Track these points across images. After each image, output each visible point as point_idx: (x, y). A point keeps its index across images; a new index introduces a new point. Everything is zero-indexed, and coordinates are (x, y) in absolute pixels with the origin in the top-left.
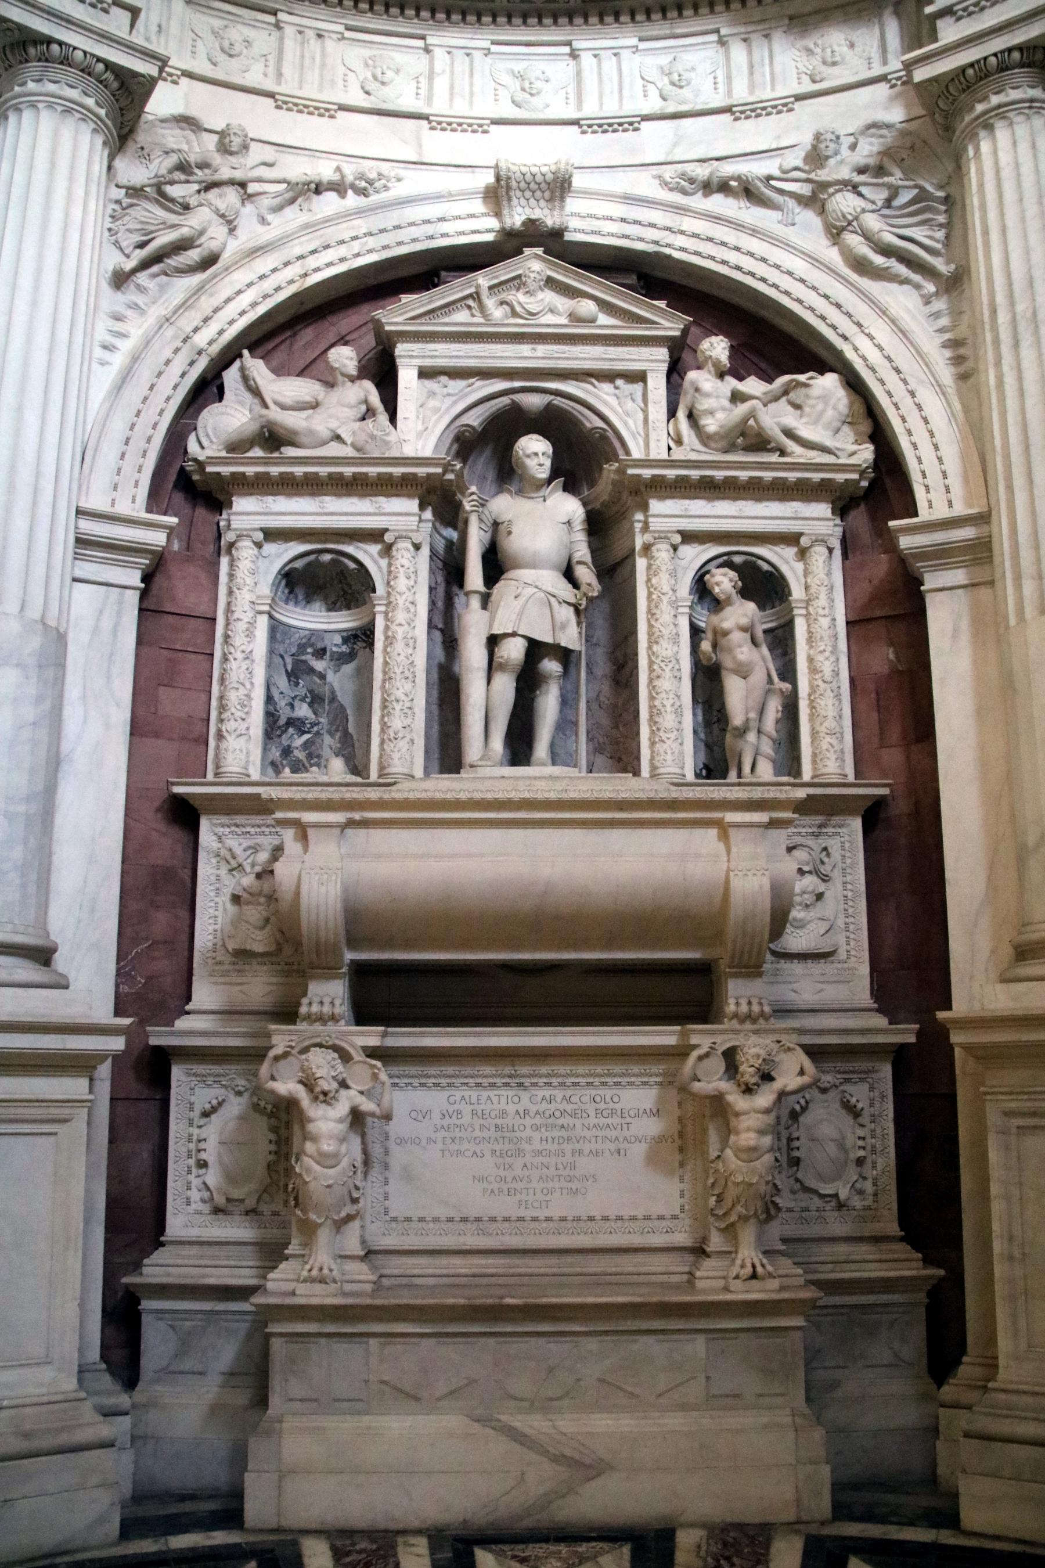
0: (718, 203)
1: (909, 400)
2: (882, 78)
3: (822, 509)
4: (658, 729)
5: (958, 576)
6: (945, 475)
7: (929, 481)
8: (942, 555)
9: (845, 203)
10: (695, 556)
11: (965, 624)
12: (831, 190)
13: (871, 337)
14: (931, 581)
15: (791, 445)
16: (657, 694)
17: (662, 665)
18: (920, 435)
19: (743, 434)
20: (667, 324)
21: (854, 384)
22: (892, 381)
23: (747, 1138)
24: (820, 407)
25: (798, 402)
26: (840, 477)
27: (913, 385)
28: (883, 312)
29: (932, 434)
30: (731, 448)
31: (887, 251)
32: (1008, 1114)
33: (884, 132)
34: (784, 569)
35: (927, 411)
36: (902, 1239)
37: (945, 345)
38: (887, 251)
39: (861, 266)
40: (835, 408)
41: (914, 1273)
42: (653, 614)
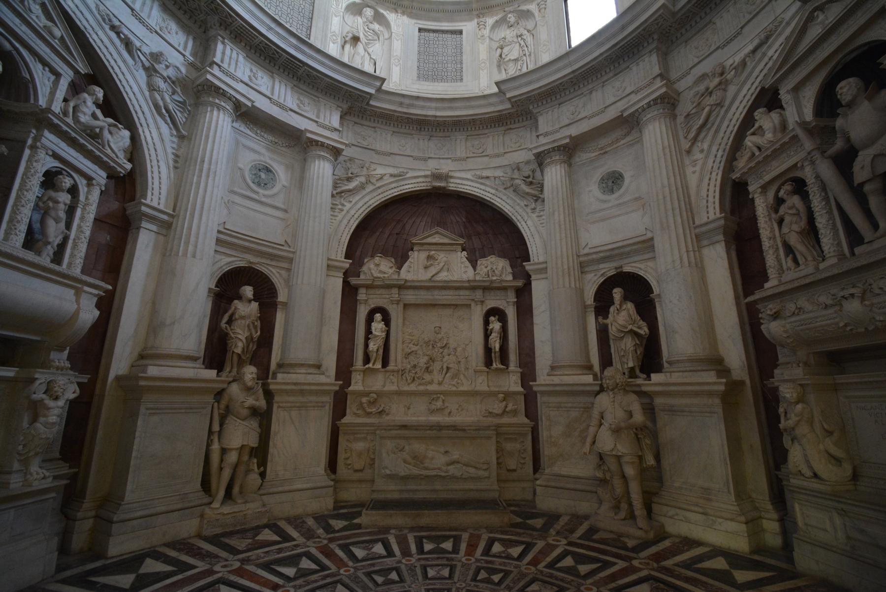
0: (113, 35)
1: (156, 161)
2: (184, 56)
3: (104, 174)
4: (16, 229)
5: (154, 228)
6: (160, 194)
7: (154, 192)
8: (152, 219)
9: (162, 85)
10: (54, 164)
11: (151, 244)
12: (158, 75)
13: (151, 133)
14: (144, 224)
15: (107, 147)
16: (20, 213)
17: (27, 202)
18: (156, 175)
19: (91, 130)
20: (81, 66)
21: (135, 139)
22: (152, 152)
23: (53, 419)
24: (120, 139)
25: (113, 132)
26: (119, 169)
27: (159, 158)
28: (158, 128)
29: (160, 178)
30: (84, 131)
31: (168, 111)
32: (147, 409)
33: (179, 72)
34: (80, 187)
35: (161, 170)
36: (59, 459)
37: (173, 154)
38: (168, 111)
39: (157, 107)
40: (124, 143)
41: (66, 472)
42: (29, 178)
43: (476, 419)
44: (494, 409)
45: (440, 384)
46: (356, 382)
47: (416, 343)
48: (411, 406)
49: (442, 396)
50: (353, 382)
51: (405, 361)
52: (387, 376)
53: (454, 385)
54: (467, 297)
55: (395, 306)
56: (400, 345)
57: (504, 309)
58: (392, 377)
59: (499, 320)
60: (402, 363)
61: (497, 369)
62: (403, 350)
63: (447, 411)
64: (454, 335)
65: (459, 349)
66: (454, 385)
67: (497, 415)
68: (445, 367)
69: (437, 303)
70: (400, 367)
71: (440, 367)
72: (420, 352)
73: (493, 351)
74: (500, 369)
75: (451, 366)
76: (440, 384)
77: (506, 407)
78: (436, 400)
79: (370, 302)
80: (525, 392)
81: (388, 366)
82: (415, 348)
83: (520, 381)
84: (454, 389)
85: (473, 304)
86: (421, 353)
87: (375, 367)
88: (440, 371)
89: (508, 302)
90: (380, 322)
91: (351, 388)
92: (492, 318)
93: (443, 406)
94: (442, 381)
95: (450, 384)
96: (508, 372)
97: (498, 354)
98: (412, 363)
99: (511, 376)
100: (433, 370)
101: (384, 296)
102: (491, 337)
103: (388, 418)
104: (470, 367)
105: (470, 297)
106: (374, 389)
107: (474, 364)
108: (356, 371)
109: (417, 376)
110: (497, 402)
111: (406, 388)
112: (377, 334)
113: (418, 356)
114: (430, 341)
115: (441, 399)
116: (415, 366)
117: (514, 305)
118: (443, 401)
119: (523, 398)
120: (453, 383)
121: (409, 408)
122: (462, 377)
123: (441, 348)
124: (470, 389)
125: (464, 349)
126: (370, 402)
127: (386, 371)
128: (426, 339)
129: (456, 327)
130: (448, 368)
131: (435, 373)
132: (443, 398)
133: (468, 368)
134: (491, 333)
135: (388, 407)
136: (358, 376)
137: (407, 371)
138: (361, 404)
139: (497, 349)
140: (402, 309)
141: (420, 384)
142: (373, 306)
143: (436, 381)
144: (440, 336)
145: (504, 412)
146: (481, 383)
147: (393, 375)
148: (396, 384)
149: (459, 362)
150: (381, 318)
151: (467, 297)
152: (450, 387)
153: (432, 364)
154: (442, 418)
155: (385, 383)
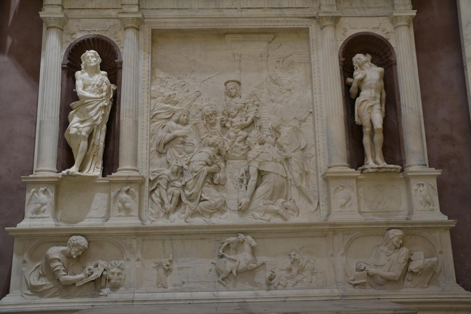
43: (337, 292)
44: (376, 266)
45: (242, 210)
46: (37, 212)
47: (183, 118)
48: (175, 266)
49: (249, 238)
50: (29, 211)
51: (157, 160)
52: (113, 194)
53: (277, 213)
54: (299, 12)
55: (131, 34)
56: (143, 121)
57: (385, 36)
58: (124, 196)
59: (376, 61)
60: (150, 164)
61: (378, 171)
62: (151, 135)
63: (262, 277)
64: (273, 101)
65: (285, 130)
66: (277, 213)
67: (389, 281)
68: (253, 171)
69: (231, 26)
70: (145, 171)
71: (243, 171)
72: (193, 139)
73: (367, 130)
74: (387, 172)
75: (266, 168)
76: (242, 210)
77: (409, 261)
78: (236, 250)
79: (72, 25)
80: (453, 223)
81: (116, 171)
82: (180, 130)
83: (436, 199)
84: (278, 220)
85: (313, 28)
86: (195, 142)
87: (85, 173)
88: (242, 181)
89: (394, 20)
90: (93, 71)
91: (24, 224)
92: (359, 58)
93: (255, 261)
94: (249, 204)
95: (266, 212)
96: (407, 180)
97: (379, 138)
98: (174, 163)
99: (414, 187)
100: (225, 179)
101: (105, 13)
102: (358, 101)
103: (115, 296)
104: (312, 171)
105: (308, 13)
106: (85, 223)
107: (323, 164)
108: (38, 183)
109: (188, 193)
110: (385, 249)
111: (162, 222)
112: (87, 94)
113: (188, 149)
114: (215, 113)
115: (247, 247)
116: (180, 172)
117: (409, 26)
118: (253, 250)
119: (447, 237)
120: (276, 208)
121: (168, 271)
122: (294, 193)
123: (244, 128)
124: (315, 219)
125: (297, 130)
126: (69, 257)
127: (111, 183)
128: (207, 109)
129: (275, 82)
130: (261, 174)
131: (230, 185)
132: (254, 243)
133: (307, 173)
134: (359, 91)
135: (115, 270)
136: (43, 197)
137: (163, 183)
138: (48, 261)
139: (378, 123)
140: (149, 42)
141: (195, 213)
142: (79, 36)
143: (232, 204)
144: (238, 102)
145: (406, 271)
146: (343, 206)
147: (127, 192)
148: (135, 213)
149: (287, 159)
150: (99, 60)
151: (299, 12)
152: (268, 217)
153: (222, 165)
154: (249, 292)
155: (109, 211)
